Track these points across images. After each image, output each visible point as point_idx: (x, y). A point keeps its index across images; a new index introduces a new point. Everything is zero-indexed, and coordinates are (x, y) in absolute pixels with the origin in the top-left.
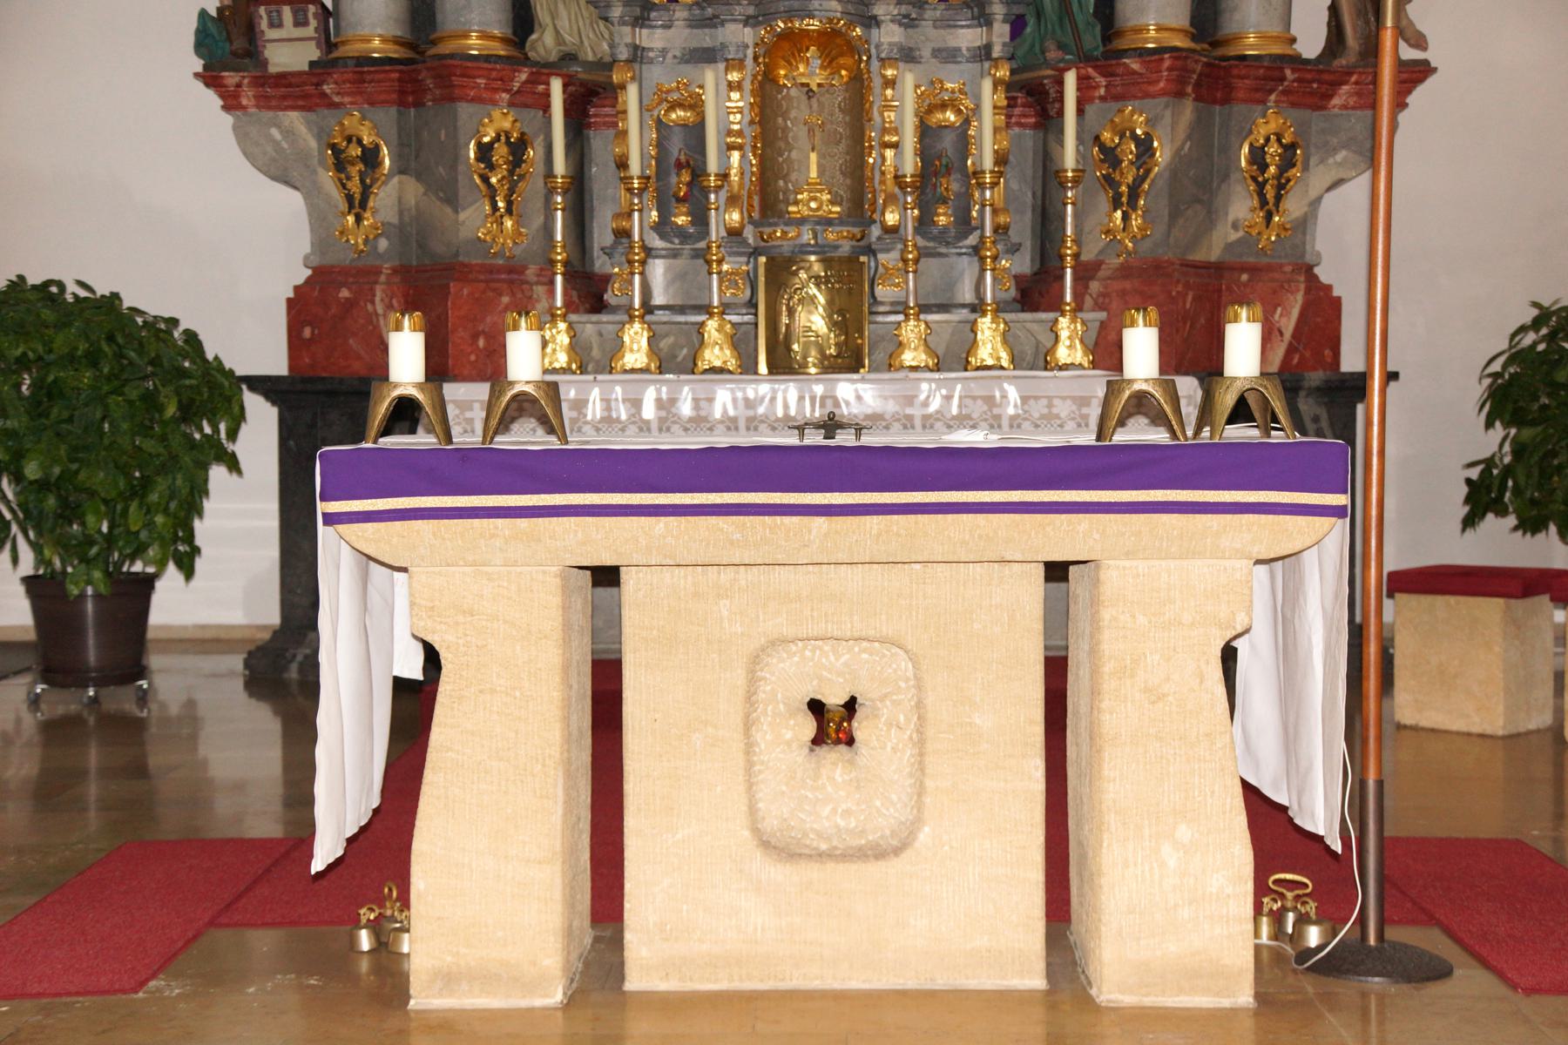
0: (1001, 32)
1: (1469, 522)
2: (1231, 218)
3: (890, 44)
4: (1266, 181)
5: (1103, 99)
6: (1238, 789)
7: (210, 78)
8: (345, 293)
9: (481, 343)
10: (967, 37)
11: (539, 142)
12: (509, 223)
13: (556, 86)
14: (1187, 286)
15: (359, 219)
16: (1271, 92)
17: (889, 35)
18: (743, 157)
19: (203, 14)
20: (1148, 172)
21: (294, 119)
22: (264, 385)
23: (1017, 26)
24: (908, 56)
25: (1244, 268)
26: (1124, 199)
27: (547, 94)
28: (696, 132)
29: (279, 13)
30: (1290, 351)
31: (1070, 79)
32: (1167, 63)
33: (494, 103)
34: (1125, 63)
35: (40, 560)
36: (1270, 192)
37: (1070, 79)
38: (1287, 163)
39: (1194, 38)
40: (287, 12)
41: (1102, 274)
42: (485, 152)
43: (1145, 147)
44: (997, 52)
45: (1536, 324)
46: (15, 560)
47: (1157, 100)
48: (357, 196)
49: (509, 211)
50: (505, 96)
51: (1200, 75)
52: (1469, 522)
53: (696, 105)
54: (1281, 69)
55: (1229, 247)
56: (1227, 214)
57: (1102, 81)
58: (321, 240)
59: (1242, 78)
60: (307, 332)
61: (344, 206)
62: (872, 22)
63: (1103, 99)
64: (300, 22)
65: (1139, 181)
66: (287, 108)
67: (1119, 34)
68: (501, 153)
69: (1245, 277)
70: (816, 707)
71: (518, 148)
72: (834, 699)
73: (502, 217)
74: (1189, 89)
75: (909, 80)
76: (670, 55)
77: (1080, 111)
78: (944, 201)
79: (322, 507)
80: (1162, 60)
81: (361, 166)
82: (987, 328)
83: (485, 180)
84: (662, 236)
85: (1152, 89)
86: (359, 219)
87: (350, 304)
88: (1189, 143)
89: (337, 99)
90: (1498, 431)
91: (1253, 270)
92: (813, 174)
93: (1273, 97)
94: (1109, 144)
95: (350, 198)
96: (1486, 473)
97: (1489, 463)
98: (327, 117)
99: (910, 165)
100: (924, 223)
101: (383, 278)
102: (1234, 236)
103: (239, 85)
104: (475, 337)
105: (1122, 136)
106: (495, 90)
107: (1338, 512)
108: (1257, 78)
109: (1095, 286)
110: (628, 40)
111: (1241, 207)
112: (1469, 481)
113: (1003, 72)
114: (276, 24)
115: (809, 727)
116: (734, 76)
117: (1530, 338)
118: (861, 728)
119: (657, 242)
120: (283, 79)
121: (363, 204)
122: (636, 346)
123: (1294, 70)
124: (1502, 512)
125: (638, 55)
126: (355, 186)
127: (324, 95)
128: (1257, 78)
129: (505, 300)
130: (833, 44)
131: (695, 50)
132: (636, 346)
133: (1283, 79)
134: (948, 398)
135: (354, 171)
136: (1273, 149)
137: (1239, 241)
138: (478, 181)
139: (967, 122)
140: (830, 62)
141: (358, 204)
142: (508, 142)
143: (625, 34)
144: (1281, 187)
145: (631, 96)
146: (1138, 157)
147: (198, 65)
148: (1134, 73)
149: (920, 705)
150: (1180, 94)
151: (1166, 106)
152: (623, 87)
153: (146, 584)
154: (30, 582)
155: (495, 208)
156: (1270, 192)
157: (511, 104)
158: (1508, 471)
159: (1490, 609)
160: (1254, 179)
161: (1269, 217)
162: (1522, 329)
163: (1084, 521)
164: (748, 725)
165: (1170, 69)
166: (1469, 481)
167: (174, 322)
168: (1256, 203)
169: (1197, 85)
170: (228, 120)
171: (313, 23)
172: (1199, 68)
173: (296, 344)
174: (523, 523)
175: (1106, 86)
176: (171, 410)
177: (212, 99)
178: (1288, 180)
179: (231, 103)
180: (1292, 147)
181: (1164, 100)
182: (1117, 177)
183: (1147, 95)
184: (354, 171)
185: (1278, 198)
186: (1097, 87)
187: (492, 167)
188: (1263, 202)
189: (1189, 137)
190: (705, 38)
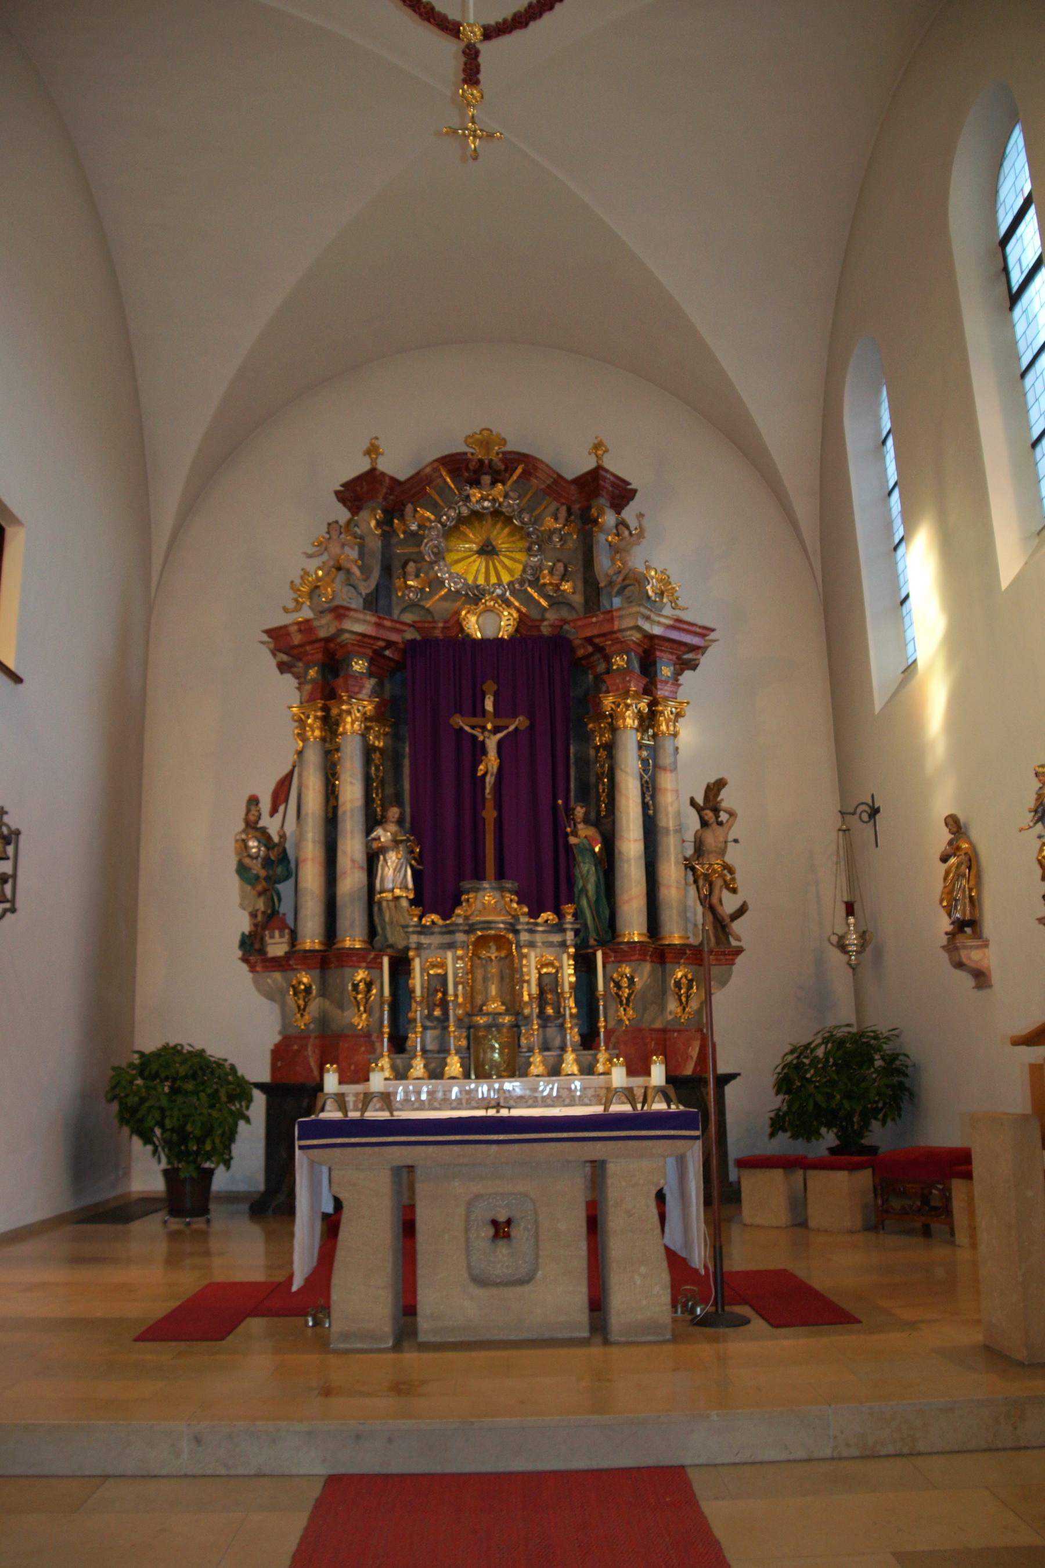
0: (570, 936)
1: (772, 1135)
2: (669, 1010)
3: (525, 941)
4: (682, 995)
5: (613, 962)
6: (663, 1251)
7: (245, 960)
8: (295, 1047)
9: (352, 1067)
10: (556, 938)
11: (378, 982)
12: (364, 1016)
13: (386, 961)
14: (652, 1039)
15: (302, 1015)
16: (681, 958)
17: (524, 937)
18: (464, 988)
19: (243, 934)
20: (633, 992)
21: (277, 975)
22: (260, 1086)
23: (577, 932)
24: (532, 945)
25: (675, 1031)
26: (625, 1001)
27: (381, 963)
28: (444, 978)
29: (273, 933)
30: (696, 1065)
31: (599, 955)
32: (638, 948)
33: (360, 967)
34: (622, 948)
35: (169, 1162)
36: (684, 999)
37: (599, 955)
38: (690, 987)
39: (650, 937)
40: (277, 933)
41: (616, 1034)
42: (355, 987)
43: (631, 980)
44: (569, 943)
45: (792, 1052)
46: (159, 1161)
47: (633, 963)
48: (302, 1007)
49: (365, 1011)
50: (364, 964)
51: (652, 952)
52: (772, 1135)
53: (443, 965)
54: (685, 950)
55: (668, 1022)
56: (666, 1008)
57: (613, 954)
58: (285, 1025)
59: (670, 953)
60: (279, 1064)
61: (297, 1010)
62: (516, 932)
63: (613, 962)
64: (282, 936)
65: (630, 995)
66: (274, 971)
67: (619, 936)
68: (362, 986)
69: (676, 1034)
70: (495, 1223)
71: (369, 985)
72: (502, 1218)
73: (362, 1014)
74: (648, 958)
75: (533, 955)
76: (433, 946)
77: (604, 966)
78: (549, 1004)
79: (297, 1143)
80: (635, 947)
81: (304, 994)
82: (570, 1057)
83: (355, 998)
84: (431, 1021)
85: (633, 958)
86: (302, 1015)
87: (299, 1051)
88: (649, 980)
89: (295, 967)
90: (780, 1097)
91: (679, 1031)
92: (494, 993)
93: (682, 961)
94: (617, 980)
95: (299, 1007)
96: (777, 1115)
97: (779, 1110)
98: (290, 974)
99: (535, 990)
100: (542, 1014)
101: (311, 1040)
102: (670, 1017)
103: (256, 963)
104: (350, 1065)
105: (622, 977)
106: (360, 962)
107: (696, 1138)
108: (675, 953)
109: (613, 1039)
110: (415, 940)
111: (672, 1006)
112: (771, 1119)
113: (572, 950)
114: (272, 937)
115: (491, 1231)
116: (460, 953)
117: (790, 1058)
118: (514, 1233)
119: (428, 1024)
120: (275, 960)
121: (304, 1010)
122: (418, 1067)
123: (690, 950)
124: (785, 1131)
125: (419, 947)
126: (301, 1002)
127: (290, 965)
128: (675, 953)
129: (363, 1049)
130: (500, 941)
131: (442, 944)
132: (418, 1067)
133: (685, 953)
134: (552, 1089)
135: (301, 996)
136: (684, 980)
137: (672, 1020)
138: (352, 999)
139: (557, 972)
140: (498, 949)
141: (302, 1010)
142: (365, 983)
143: (414, 939)
144: (688, 997)
145: (417, 964)
146: (629, 985)
147: (239, 954)
148: (625, 951)
149: (536, 1221)
150: (645, 960)
151: (639, 965)
152: (413, 959)
153: (210, 1172)
154: (166, 1173)
155: (359, 1010)
156: (684, 999)
157: (367, 968)
158: (785, 1114)
159: (778, 1174)
160: (677, 994)
161: (684, 1009)
162: (786, 1054)
163: (599, 1145)
164: (467, 1230)
165: (640, 950)
166: (771, 1119)
167: (226, 1060)
168: (679, 1004)
169: (651, 956)
170: (250, 975)
171: (287, 936)
172: (651, 949)
173: (274, 1069)
174: (376, 1149)
175: (615, 957)
176: (224, 1099)
177: (245, 967)
178: (691, 994)
179: (252, 969)
180: (691, 981)
181: (637, 962)
182: (620, 993)
183: (631, 961)
184: (301, 996)
185: (687, 1001)
186: (610, 957)
187: (358, 993)
188: (681, 1003)
189: (649, 977)
190: (447, 939)
